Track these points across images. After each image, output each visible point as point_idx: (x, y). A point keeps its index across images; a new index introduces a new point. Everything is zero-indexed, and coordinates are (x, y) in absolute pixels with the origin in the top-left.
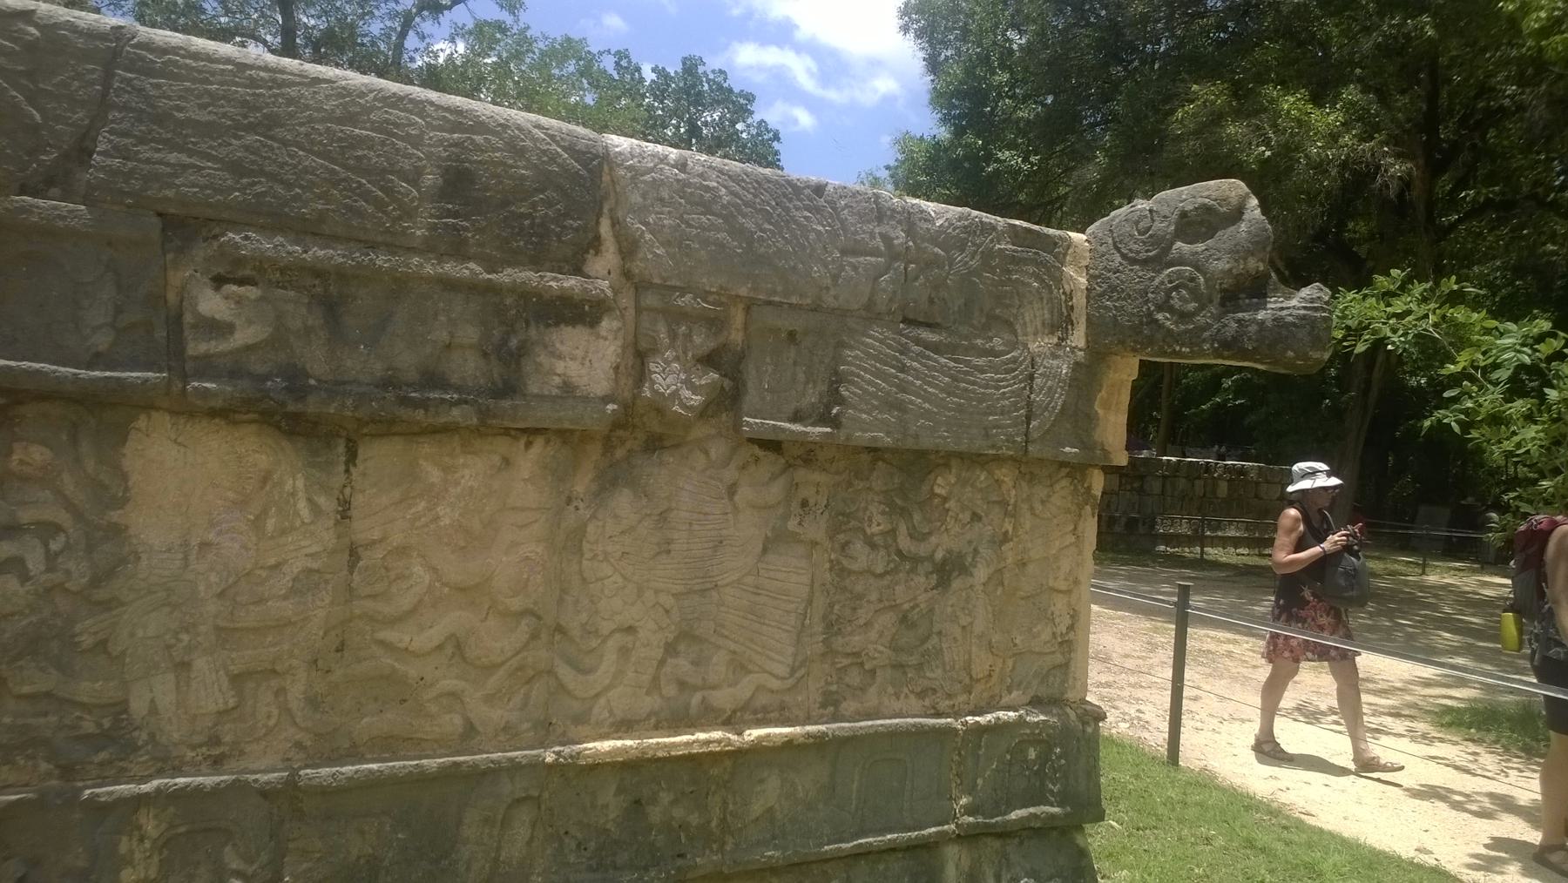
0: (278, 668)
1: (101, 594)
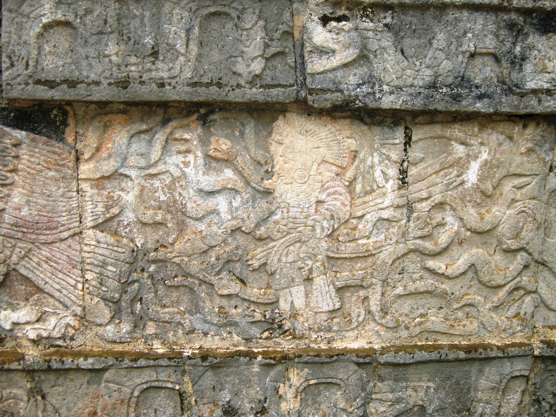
0: (364, 284)
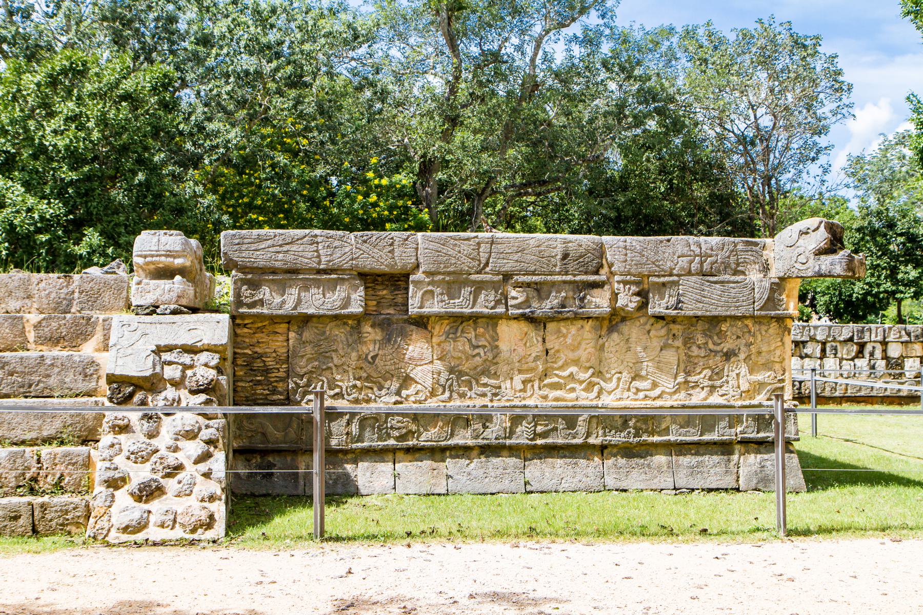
1: (495, 361)
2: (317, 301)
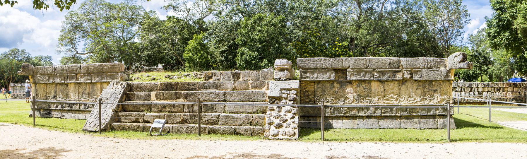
2: (322, 77)
